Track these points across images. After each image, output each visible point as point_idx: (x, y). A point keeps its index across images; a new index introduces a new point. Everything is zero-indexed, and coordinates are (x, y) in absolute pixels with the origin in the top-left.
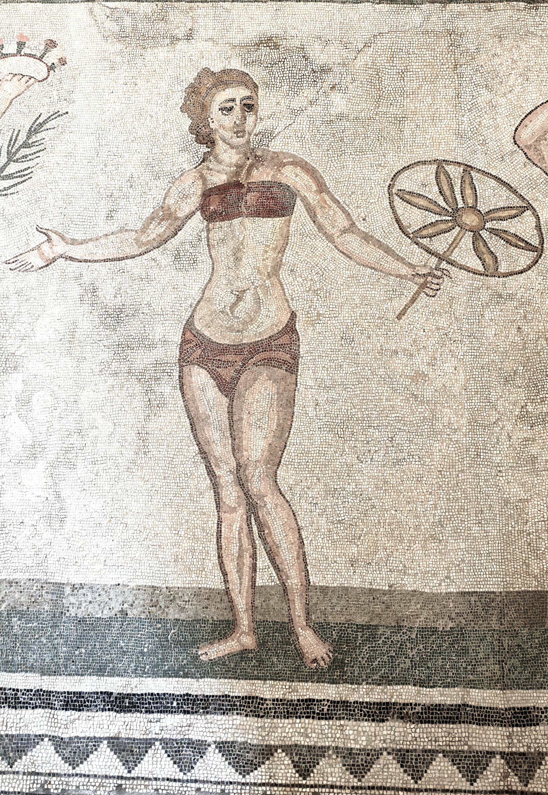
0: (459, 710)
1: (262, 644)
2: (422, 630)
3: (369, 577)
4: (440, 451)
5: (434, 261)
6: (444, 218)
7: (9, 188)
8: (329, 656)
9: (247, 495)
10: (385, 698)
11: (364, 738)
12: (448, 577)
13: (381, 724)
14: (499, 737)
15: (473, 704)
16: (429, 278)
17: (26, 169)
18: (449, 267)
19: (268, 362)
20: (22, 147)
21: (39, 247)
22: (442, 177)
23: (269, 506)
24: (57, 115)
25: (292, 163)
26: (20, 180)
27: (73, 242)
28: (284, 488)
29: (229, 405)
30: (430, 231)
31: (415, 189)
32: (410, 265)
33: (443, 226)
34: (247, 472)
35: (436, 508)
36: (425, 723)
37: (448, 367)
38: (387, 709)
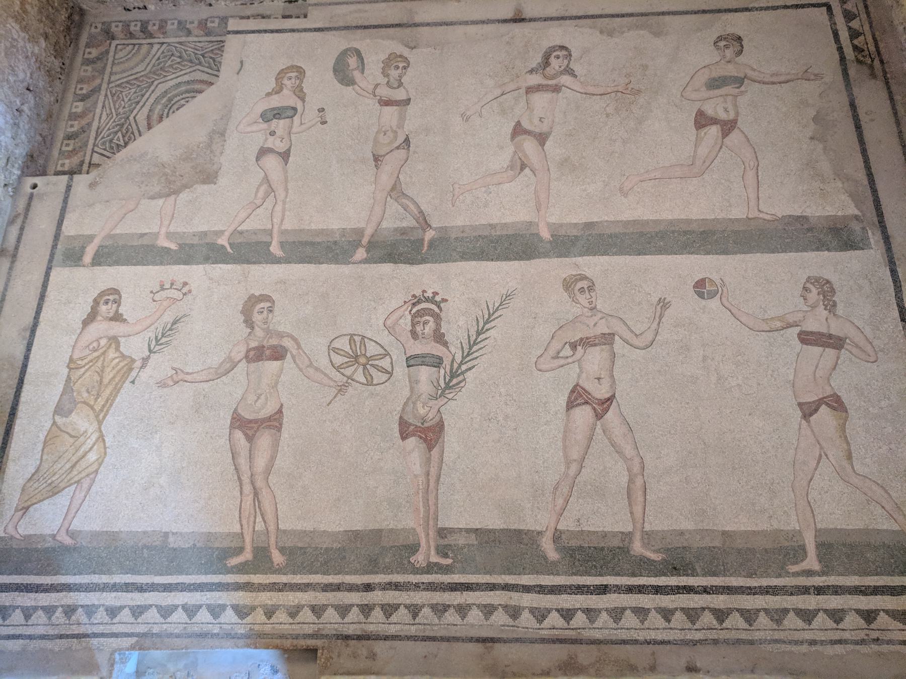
1: (255, 557)
2: (326, 549)
3: (305, 525)
5: (345, 379)
19: (269, 427)
20: (169, 330)
21: (172, 376)
24: (185, 316)
27: (188, 373)
28: (271, 485)
32: (335, 381)
33: (350, 363)
37: (348, 427)
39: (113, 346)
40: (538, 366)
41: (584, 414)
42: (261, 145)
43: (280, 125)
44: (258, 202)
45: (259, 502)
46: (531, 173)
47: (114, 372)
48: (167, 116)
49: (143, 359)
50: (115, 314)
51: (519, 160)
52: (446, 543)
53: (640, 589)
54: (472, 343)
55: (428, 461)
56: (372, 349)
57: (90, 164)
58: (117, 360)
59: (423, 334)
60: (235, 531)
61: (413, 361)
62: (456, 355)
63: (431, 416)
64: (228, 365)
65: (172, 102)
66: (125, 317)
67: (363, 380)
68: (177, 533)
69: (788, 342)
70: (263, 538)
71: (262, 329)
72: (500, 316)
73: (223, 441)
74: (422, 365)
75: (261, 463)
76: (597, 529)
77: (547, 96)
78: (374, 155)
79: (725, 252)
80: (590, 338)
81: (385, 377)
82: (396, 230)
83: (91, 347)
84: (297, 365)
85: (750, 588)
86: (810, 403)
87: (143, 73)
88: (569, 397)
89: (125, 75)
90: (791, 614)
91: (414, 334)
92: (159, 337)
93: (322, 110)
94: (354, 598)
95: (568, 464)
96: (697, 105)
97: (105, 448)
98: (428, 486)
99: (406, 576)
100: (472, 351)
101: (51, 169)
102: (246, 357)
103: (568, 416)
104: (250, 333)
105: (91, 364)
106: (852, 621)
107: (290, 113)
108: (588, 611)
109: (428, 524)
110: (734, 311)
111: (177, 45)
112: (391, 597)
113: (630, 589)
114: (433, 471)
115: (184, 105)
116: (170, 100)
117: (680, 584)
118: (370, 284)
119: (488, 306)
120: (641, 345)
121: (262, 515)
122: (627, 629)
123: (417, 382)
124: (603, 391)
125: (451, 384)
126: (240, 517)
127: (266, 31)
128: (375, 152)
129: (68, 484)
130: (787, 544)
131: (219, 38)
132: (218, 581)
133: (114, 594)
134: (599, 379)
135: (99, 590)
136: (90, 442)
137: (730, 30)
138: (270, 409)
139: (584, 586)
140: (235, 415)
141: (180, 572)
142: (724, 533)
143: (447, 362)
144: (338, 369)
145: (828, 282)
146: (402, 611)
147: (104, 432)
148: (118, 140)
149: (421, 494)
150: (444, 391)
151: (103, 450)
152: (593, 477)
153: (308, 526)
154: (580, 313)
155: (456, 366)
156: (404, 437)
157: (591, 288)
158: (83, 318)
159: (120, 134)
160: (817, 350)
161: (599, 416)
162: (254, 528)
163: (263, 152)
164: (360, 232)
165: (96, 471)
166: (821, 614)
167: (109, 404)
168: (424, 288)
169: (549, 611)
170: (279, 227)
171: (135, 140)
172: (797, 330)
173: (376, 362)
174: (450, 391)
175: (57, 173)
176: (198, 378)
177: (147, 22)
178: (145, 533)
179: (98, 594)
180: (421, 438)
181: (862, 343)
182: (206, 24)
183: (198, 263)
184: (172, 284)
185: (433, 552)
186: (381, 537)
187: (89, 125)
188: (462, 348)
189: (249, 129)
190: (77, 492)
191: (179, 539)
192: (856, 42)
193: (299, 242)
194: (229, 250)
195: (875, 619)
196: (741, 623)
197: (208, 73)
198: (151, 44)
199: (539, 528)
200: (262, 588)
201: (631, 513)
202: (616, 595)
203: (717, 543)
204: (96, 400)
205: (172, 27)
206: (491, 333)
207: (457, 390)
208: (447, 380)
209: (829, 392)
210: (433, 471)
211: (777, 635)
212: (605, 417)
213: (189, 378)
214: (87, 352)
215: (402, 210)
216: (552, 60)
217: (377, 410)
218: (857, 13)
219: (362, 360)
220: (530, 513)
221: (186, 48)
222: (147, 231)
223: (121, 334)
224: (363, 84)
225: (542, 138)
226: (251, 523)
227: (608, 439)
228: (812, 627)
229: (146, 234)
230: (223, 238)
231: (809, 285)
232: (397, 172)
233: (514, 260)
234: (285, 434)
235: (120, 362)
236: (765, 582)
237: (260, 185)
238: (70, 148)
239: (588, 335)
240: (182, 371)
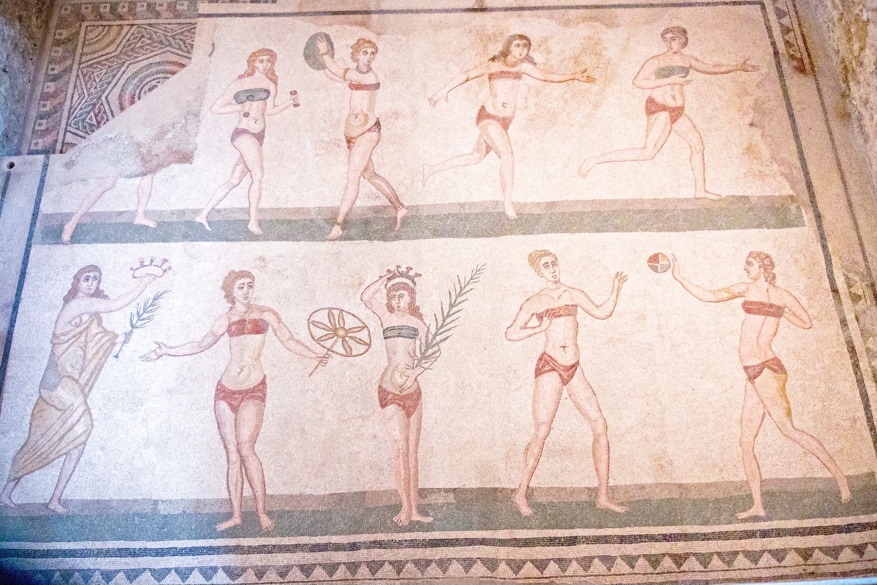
5: (326, 350)
12: (325, 487)
15: (333, 542)
16: (323, 359)
19: (252, 397)
23: (250, 461)
24: (166, 292)
26: (148, 321)
27: (171, 348)
28: (257, 452)
30: (325, 338)
33: (330, 336)
35: (321, 458)
40: (508, 336)
41: (551, 380)
42: (236, 125)
43: (254, 107)
44: (235, 181)
45: (246, 469)
47: (98, 346)
48: (139, 98)
50: (96, 291)
51: (484, 144)
52: (426, 503)
53: (606, 540)
54: (445, 315)
55: (408, 426)
56: (350, 323)
57: (63, 143)
58: (100, 336)
59: (399, 307)
61: (388, 333)
63: (408, 384)
65: (144, 83)
66: (106, 293)
67: (343, 352)
68: (166, 501)
69: (733, 311)
70: (251, 503)
72: (471, 289)
73: (209, 412)
76: (566, 486)
77: (510, 82)
78: (346, 137)
79: (675, 229)
80: (555, 310)
81: (363, 348)
82: (369, 208)
83: (73, 323)
84: (279, 338)
85: (705, 535)
86: (753, 366)
87: (113, 54)
88: (537, 365)
89: (96, 55)
90: (741, 556)
91: (391, 309)
92: (141, 312)
93: (294, 93)
94: (341, 557)
95: (538, 426)
96: (647, 93)
97: (92, 420)
98: (408, 450)
99: (390, 534)
100: (446, 323)
101: (25, 148)
102: (228, 331)
103: (537, 382)
104: (231, 308)
105: (74, 339)
106: (792, 558)
107: (264, 95)
108: (559, 561)
109: (409, 485)
110: (685, 283)
111: (147, 27)
112: (377, 554)
113: (597, 540)
114: (412, 437)
115: (156, 86)
116: (141, 81)
117: (642, 534)
118: (346, 260)
119: (459, 280)
120: (602, 315)
121: (249, 481)
122: (596, 576)
124: (569, 358)
125: (426, 355)
126: (228, 484)
127: (236, 15)
128: (347, 135)
129: (57, 456)
130: (736, 494)
131: (188, 21)
132: (208, 545)
133: (108, 559)
134: (564, 347)
135: (94, 556)
136: (76, 416)
137: (676, 23)
138: (254, 380)
139: (555, 538)
142: (680, 486)
143: (422, 334)
144: (318, 341)
145: (768, 256)
146: (387, 567)
147: (90, 405)
148: (91, 119)
149: (401, 457)
150: (420, 361)
151: (89, 422)
152: (561, 438)
153: (295, 490)
154: (545, 286)
155: (430, 337)
156: (383, 406)
157: (554, 264)
158: (64, 295)
159: (92, 114)
160: (760, 318)
161: (565, 382)
163: (238, 133)
164: (335, 212)
165: (85, 443)
166: (766, 555)
167: (94, 377)
169: (524, 562)
171: (108, 120)
172: (740, 301)
174: (427, 361)
175: (31, 153)
176: (181, 352)
177: (118, 4)
179: (92, 559)
180: (399, 405)
181: (799, 312)
182: (175, 7)
183: (176, 241)
184: (152, 261)
185: (414, 511)
186: (364, 499)
187: (61, 104)
188: (436, 320)
189: (223, 110)
190: (67, 463)
191: (169, 506)
192: (786, 37)
193: (277, 220)
194: (208, 228)
195: (811, 556)
196: (698, 566)
197: (179, 55)
198: (121, 26)
199: (512, 486)
200: (251, 550)
201: (597, 470)
202: (585, 545)
203: (676, 495)
205: (141, 9)
207: (433, 360)
208: (423, 351)
209: (770, 356)
210: (412, 437)
211: (728, 575)
212: (570, 382)
213: (172, 352)
214: (69, 327)
215: (374, 190)
216: (513, 48)
218: (787, 11)
219: (341, 333)
220: (504, 472)
221: (156, 30)
222: (125, 209)
223: (103, 310)
224: (334, 69)
225: (505, 123)
226: (239, 489)
227: (574, 403)
228: (758, 566)
229: (124, 212)
230: (201, 216)
231: (751, 259)
232: (369, 154)
233: (482, 237)
234: (269, 403)
235: (102, 337)
236: (717, 529)
237: (237, 165)
238: (43, 128)
239: (554, 307)
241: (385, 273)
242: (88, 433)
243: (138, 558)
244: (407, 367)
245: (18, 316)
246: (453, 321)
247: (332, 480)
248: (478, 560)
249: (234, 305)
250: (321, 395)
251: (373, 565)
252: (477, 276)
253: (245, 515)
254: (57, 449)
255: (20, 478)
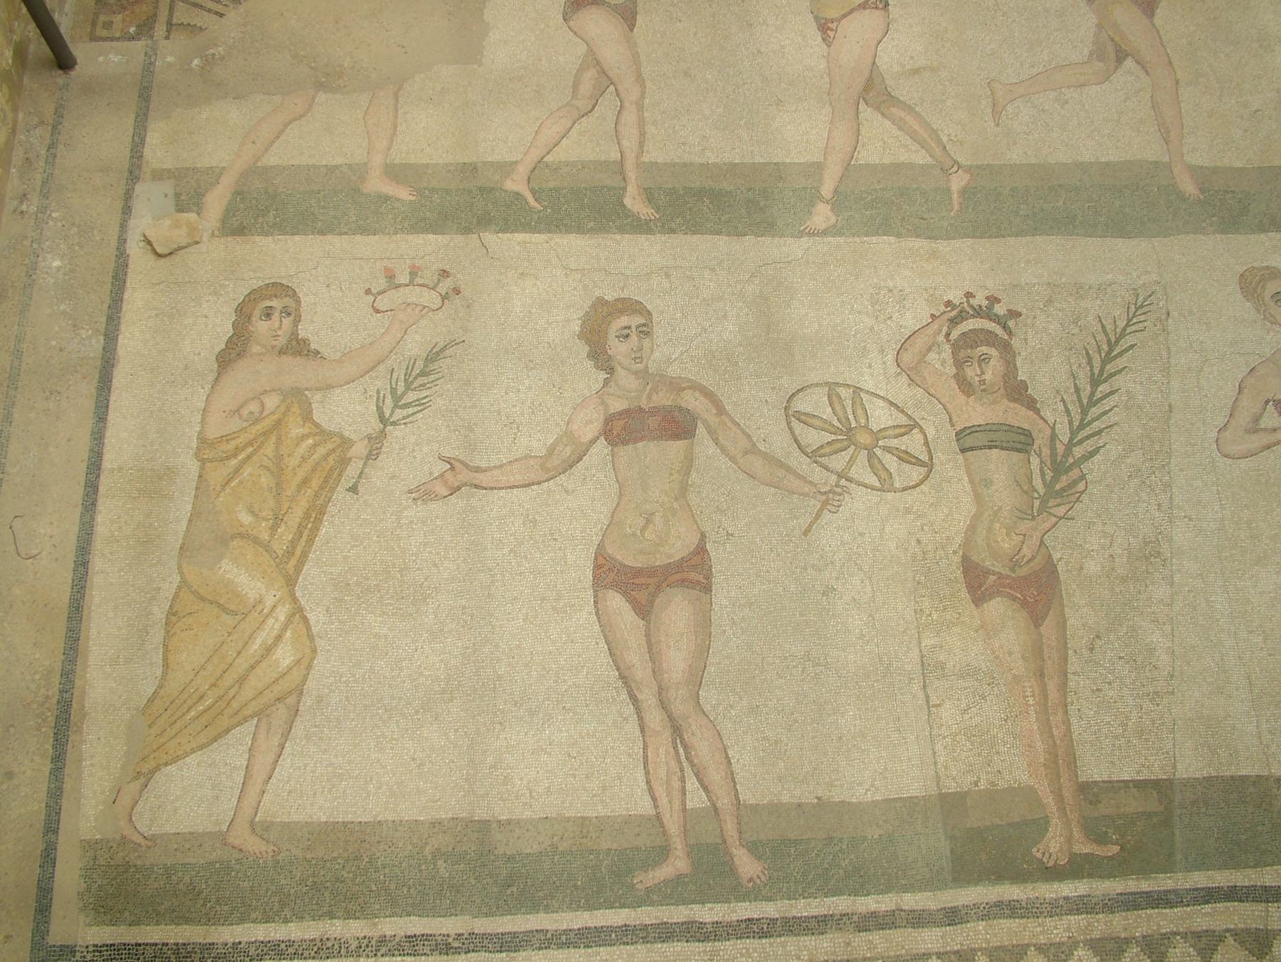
0: (894, 915)
4: (855, 662)
5: (834, 478)
6: (839, 437)
7: (408, 416)
8: (764, 874)
9: (671, 718)
10: (823, 911)
11: (805, 953)
13: (821, 937)
14: (934, 938)
16: (831, 495)
17: (425, 398)
18: (847, 484)
19: (683, 583)
21: (442, 475)
22: (834, 398)
23: (694, 727)
25: (690, 388)
27: (478, 470)
28: (707, 708)
29: (646, 627)
30: (827, 450)
31: (809, 410)
32: (811, 483)
33: (839, 445)
34: (669, 695)
36: (863, 931)
38: (825, 921)
39: (296, 409)
45: (685, 747)
46: (1138, 68)
47: (308, 466)
49: (369, 438)
50: (290, 341)
54: (1085, 401)
56: (881, 416)
59: (982, 382)
60: (641, 811)
62: (1058, 426)
63: (1026, 551)
64: (568, 450)
66: (313, 346)
71: (636, 373)
72: (1132, 347)
73: (586, 615)
74: (990, 448)
75: (677, 661)
81: (916, 473)
83: (245, 412)
84: (724, 450)
91: (966, 386)
92: (400, 390)
97: (311, 637)
104: (606, 382)
119: (1103, 327)
121: (697, 775)
123: (988, 483)
125: (1058, 487)
126: (648, 782)
136: (273, 625)
138: (678, 546)
140: (601, 561)
141: (534, 907)
143: (1041, 440)
144: (815, 455)
150: (1044, 501)
155: (1060, 449)
156: (978, 601)
158: (217, 349)
162: (684, 804)
167: (305, 538)
168: (967, 289)
170: (637, 158)
173: (894, 443)
178: (435, 824)
180: (1014, 599)
184: (413, 274)
185: (1077, 833)
188: (1067, 411)
190: (262, 736)
204: (274, 528)
206: (1119, 381)
207: (1073, 498)
208: (1048, 478)
213: (482, 479)
214: (235, 424)
217: (914, 543)
219: (863, 438)
226: (676, 794)
234: (721, 598)
235: (315, 445)
237: (581, 70)
240: (466, 466)
241: (942, 308)
242: (306, 663)
243: (456, 956)
244: (1020, 515)
245: (113, 398)
246: (1105, 413)
247: (886, 769)
248: (1227, 935)
249: (612, 374)
250: (837, 578)
251: (1003, 954)
252: (1142, 318)
253: (696, 852)
254: (235, 705)
255: (153, 772)
